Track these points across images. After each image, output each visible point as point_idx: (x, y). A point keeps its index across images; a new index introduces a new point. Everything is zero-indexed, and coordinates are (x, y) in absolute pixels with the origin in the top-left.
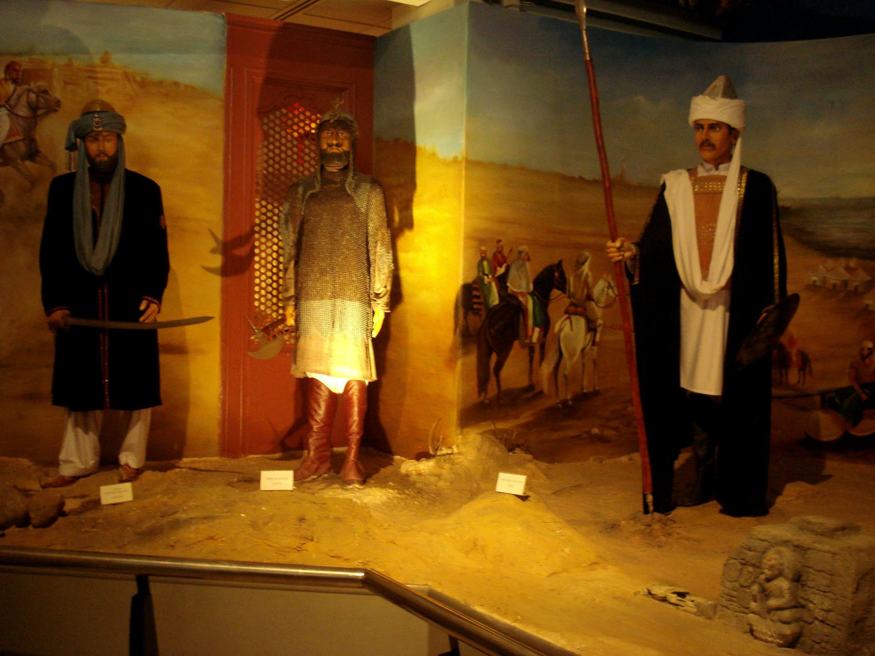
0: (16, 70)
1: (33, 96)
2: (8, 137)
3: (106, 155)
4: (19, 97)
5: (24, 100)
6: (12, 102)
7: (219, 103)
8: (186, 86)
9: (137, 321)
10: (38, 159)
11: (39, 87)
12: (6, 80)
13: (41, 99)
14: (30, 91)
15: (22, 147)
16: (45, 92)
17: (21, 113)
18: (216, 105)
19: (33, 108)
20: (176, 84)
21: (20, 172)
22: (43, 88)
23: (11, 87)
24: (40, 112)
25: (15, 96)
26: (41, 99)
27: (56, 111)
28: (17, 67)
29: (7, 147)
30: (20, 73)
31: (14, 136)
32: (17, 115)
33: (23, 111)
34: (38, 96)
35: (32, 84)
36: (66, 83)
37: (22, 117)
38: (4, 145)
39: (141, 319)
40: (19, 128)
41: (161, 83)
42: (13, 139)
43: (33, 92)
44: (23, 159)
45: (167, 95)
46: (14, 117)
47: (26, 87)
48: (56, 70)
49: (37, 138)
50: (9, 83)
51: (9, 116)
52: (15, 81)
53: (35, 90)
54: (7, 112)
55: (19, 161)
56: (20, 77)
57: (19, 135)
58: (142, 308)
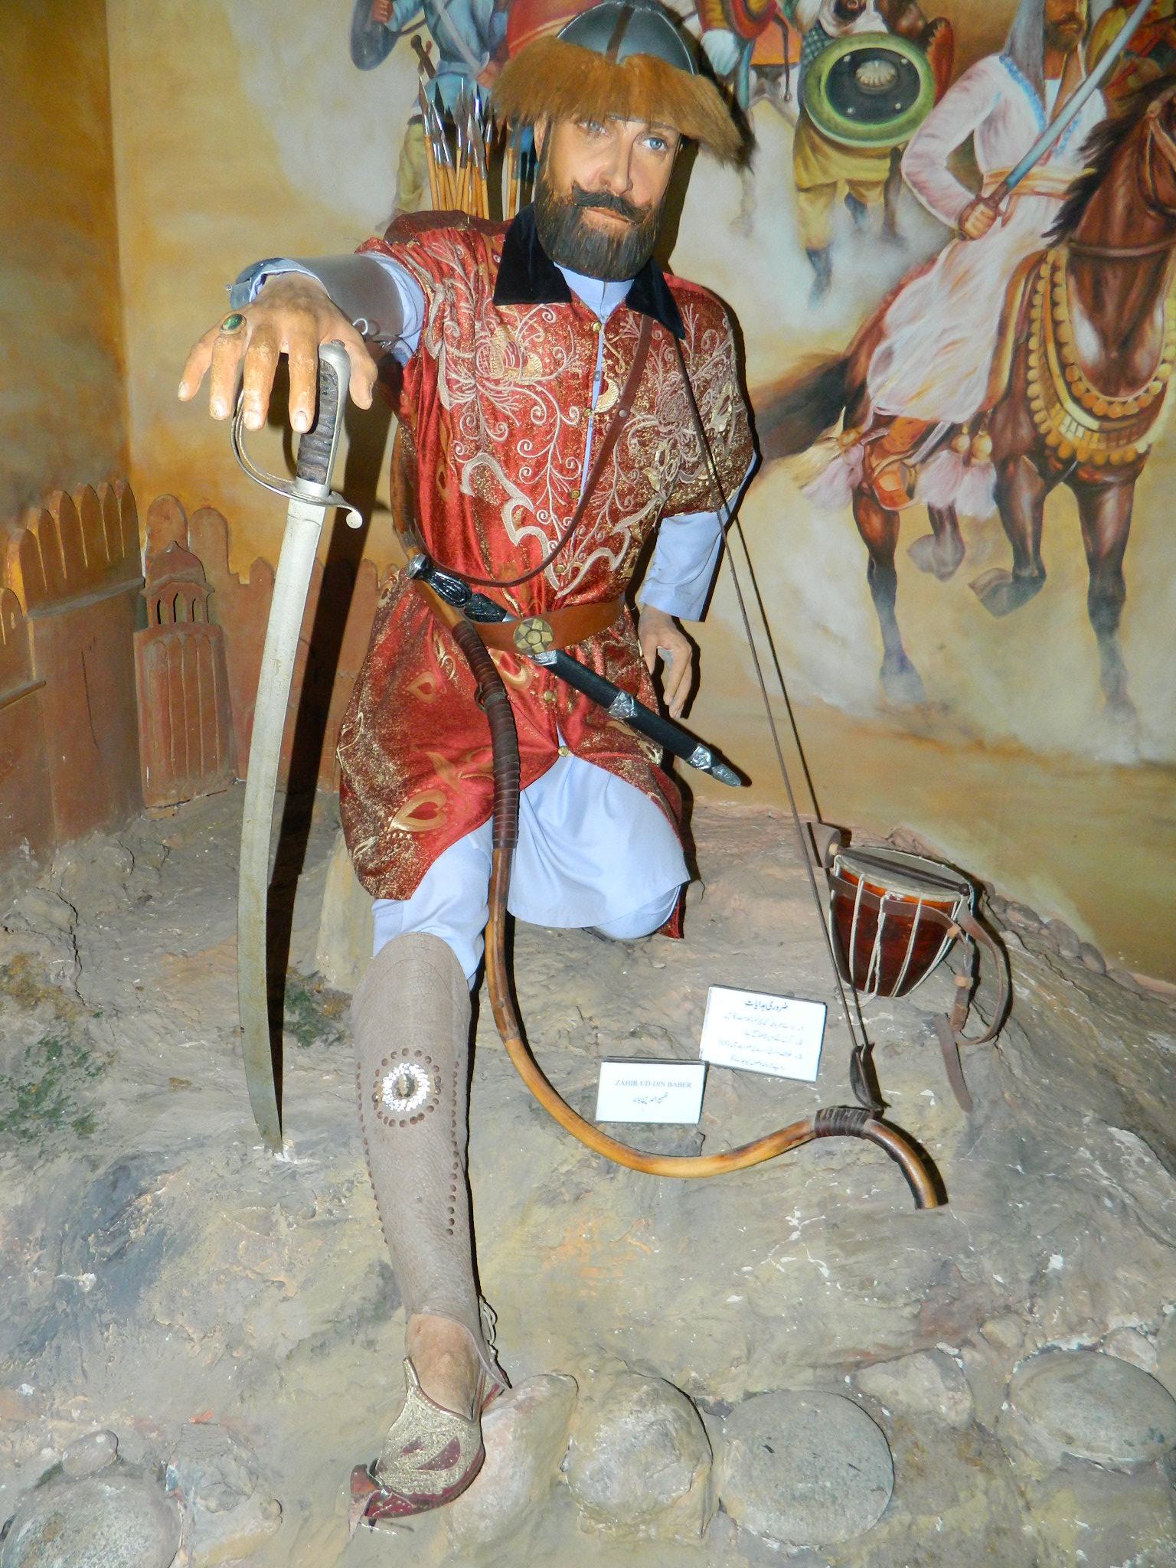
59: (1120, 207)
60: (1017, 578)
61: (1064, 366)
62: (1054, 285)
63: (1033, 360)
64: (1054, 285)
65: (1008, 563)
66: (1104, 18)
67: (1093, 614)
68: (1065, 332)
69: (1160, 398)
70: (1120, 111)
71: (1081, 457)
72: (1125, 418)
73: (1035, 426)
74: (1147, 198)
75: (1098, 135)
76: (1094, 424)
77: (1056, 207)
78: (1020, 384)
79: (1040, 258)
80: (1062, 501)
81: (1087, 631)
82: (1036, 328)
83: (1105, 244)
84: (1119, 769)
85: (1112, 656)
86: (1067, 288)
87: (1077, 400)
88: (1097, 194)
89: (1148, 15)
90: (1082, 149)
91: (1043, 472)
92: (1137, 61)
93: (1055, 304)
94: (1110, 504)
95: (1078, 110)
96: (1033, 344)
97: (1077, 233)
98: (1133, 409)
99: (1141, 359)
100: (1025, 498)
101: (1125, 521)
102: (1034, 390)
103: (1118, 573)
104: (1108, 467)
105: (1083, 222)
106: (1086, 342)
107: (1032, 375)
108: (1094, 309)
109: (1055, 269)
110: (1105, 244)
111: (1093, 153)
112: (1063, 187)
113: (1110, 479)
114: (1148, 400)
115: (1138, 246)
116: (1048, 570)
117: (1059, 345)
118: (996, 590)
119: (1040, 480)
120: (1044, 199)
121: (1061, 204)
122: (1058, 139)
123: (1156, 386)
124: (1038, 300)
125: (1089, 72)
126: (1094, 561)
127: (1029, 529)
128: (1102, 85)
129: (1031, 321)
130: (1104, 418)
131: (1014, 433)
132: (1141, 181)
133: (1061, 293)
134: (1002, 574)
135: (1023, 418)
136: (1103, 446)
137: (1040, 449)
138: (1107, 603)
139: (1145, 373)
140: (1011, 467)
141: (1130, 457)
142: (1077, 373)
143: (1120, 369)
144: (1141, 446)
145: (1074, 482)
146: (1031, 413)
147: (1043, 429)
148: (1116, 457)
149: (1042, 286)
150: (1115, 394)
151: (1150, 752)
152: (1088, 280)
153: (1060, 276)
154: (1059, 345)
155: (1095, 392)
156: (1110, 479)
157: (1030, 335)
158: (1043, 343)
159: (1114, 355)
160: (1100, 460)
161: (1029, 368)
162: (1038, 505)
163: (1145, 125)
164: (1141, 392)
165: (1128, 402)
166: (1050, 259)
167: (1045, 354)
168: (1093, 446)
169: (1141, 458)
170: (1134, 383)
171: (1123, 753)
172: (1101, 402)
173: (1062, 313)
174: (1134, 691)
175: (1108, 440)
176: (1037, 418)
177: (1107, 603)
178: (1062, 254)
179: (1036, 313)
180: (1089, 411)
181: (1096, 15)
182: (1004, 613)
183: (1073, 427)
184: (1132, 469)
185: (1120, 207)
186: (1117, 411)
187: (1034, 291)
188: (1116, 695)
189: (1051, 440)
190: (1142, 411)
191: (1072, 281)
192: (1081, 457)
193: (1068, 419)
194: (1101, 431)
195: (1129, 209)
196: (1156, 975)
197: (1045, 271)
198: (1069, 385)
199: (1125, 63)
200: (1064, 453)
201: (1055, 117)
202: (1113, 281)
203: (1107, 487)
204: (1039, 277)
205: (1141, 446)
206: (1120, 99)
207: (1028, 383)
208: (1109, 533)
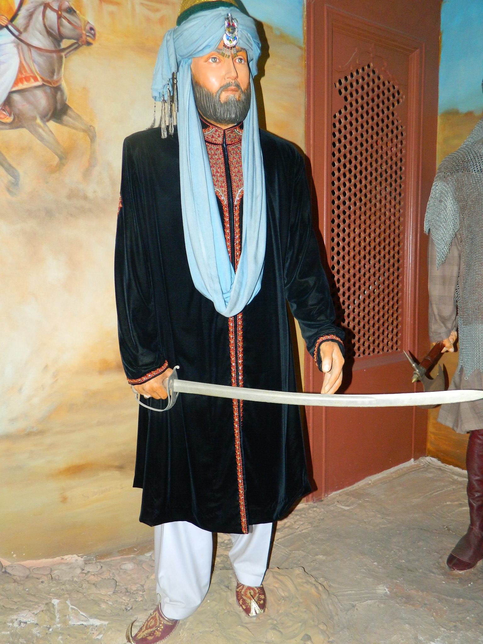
1: (52, 16)
2: (18, 80)
4: (30, 16)
6: (20, 21)
7: (299, 52)
10: (65, 118)
13: (64, 21)
15: (42, 100)
16: (70, 11)
17: (35, 43)
19: (56, 37)
21: (41, 139)
24: (65, 43)
25: (23, 13)
26: (64, 21)
27: (89, 44)
29: (16, 97)
31: (27, 79)
32: (28, 45)
33: (38, 39)
34: (59, 17)
38: (11, 93)
40: (35, 68)
44: (45, 117)
46: (25, 47)
49: (64, 85)
51: (17, 46)
54: (13, 38)
55: (39, 121)
57: (36, 79)
196: (37, 557)
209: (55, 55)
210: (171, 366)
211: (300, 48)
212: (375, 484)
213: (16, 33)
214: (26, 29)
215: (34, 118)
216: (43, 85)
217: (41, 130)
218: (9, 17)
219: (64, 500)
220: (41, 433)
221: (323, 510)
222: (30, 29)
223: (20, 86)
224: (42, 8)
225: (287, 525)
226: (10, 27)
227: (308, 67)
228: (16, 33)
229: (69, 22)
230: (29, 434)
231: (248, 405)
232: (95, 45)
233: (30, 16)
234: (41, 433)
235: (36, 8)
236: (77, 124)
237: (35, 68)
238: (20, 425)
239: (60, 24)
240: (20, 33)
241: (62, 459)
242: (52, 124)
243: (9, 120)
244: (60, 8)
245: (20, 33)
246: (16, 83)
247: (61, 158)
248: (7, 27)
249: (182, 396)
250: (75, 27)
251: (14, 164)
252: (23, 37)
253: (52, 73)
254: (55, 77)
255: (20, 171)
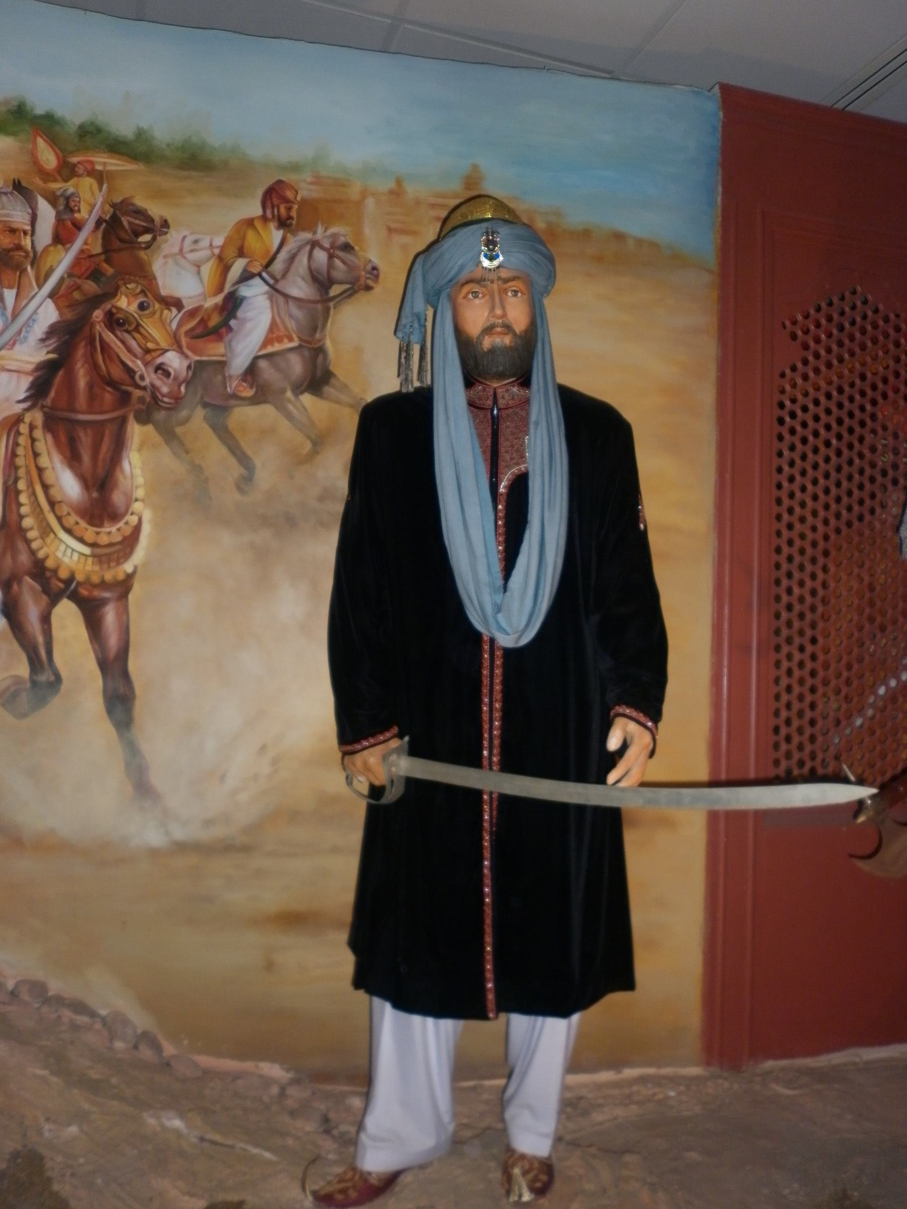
0: (286, 201)
1: (321, 256)
2: (267, 342)
3: (508, 328)
4: (292, 258)
5: (303, 260)
6: (278, 266)
8: (639, 242)
9: (601, 780)
10: (327, 389)
11: (335, 236)
12: (264, 219)
13: (337, 262)
14: (314, 244)
15: (297, 366)
16: (347, 247)
17: (295, 292)
18: (701, 284)
19: (322, 282)
20: (619, 237)
21: (289, 416)
22: (342, 240)
23: (276, 235)
24: (335, 290)
25: (283, 255)
26: (337, 262)
27: (368, 288)
28: (289, 194)
29: (263, 364)
30: (295, 207)
31: (279, 340)
32: (286, 296)
33: (299, 287)
34: (331, 257)
35: (320, 230)
36: (390, 230)
37: (297, 300)
38: (257, 358)
39: (612, 777)
41: (585, 234)
42: (277, 347)
43: (322, 248)
44: (298, 389)
45: (599, 259)
46: (281, 299)
47: (306, 236)
48: (370, 202)
49: (328, 344)
50: (272, 225)
51: (271, 298)
52: (283, 224)
53: (327, 245)
54: (266, 288)
55: (289, 394)
56: (294, 214)
57: (291, 339)
58: (613, 743)
59: (82, 382)
60: (34, 683)
61: (52, 504)
62: (33, 440)
63: (23, 498)
64: (33, 440)
65: (23, 669)
66: (46, 249)
67: (110, 711)
68: (49, 477)
69: (137, 529)
70: (69, 315)
71: (80, 577)
72: (110, 545)
73: (33, 553)
74: (102, 377)
75: (52, 331)
76: (87, 550)
77: (25, 382)
78: (14, 517)
79: (18, 419)
80: (67, 615)
81: (106, 728)
82: (22, 472)
83: (74, 410)
84: (154, 853)
85: (132, 749)
86: (45, 443)
87: (69, 531)
88: (61, 373)
89: (82, 251)
90: (43, 340)
91: (46, 590)
92: (78, 281)
93: (36, 455)
94: (110, 616)
95: (35, 312)
96: (21, 485)
97: (48, 401)
98: (118, 538)
99: (117, 498)
100: (32, 612)
101: (125, 631)
102: (27, 522)
103: (126, 675)
104: (103, 585)
105: (52, 394)
106: (69, 485)
107: (24, 510)
108: (73, 459)
109: (32, 428)
110: (74, 410)
111: (53, 343)
112: (30, 367)
113: (106, 595)
114: (128, 531)
115: (102, 413)
116: (64, 674)
117: (46, 487)
118: (15, 695)
119: (45, 599)
120: (15, 375)
121: (31, 379)
122: (20, 331)
123: (134, 520)
124: (20, 451)
125: (40, 287)
126: (103, 665)
127: (40, 639)
128: (52, 295)
129: (17, 468)
130: (93, 545)
131: (14, 557)
132: (95, 366)
133: (41, 446)
134: (18, 680)
135: (21, 545)
136: (97, 568)
137: (40, 571)
138: (120, 700)
139: (122, 509)
140: (15, 587)
141: (121, 576)
142: (65, 510)
143: (101, 505)
144: (128, 567)
145: (75, 597)
146: (28, 542)
147: (41, 554)
148: (108, 576)
149: (22, 440)
150: (101, 525)
151: (179, 834)
152: (63, 438)
153: (38, 433)
154: (46, 487)
155: (83, 524)
156: (106, 595)
157: (17, 480)
158: (30, 484)
159: (95, 495)
160: (95, 579)
161: (20, 505)
162: (46, 619)
163: (92, 326)
164: (121, 524)
165: (111, 532)
166: (28, 418)
167: (34, 494)
168: (89, 567)
169: (130, 577)
170: (115, 517)
171: (154, 837)
172: (90, 533)
173: (44, 461)
174: (157, 779)
175: (100, 563)
176: (34, 545)
177: (120, 700)
178: (38, 417)
179: (20, 461)
180: (81, 540)
181: (40, 248)
182: (24, 715)
183: (68, 553)
184: (124, 586)
185: (82, 382)
186: (104, 540)
187: (16, 444)
188: (141, 786)
189: (50, 563)
190: (125, 539)
191: (49, 437)
192: (80, 577)
193: (62, 547)
194: (93, 555)
195: (90, 387)
196: (218, 1054)
197: (24, 428)
198: (59, 519)
199: (68, 282)
200: (63, 574)
201: (15, 316)
202: (85, 440)
203: (104, 602)
204: (18, 433)
205: (128, 567)
206: (70, 306)
207: (21, 517)
208: (113, 641)
209: (319, 307)
210: (400, 736)
211: (709, 271)
212: (869, 1067)
213: (271, 282)
214: (284, 275)
215: (283, 391)
216: (300, 346)
217: (290, 407)
218: (264, 262)
219: (270, 966)
220: (246, 849)
221: (736, 1086)
222: (290, 275)
223: (270, 349)
224: (308, 248)
225: (656, 1098)
226: (264, 275)
227: (723, 300)
228: (271, 282)
229: (344, 262)
230: (225, 848)
231: (508, 803)
232: (378, 290)
233: (292, 258)
234: (246, 849)
235: (300, 249)
236: (344, 398)
237: (291, 325)
238: (218, 832)
239: (330, 265)
240: (277, 281)
241: (271, 899)
242: (307, 399)
243: (249, 393)
244: (333, 246)
245: (277, 281)
246: (264, 345)
247: (315, 444)
248: (260, 275)
249: (410, 782)
250: (351, 268)
251: (249, 452)
252: (279, 286)
253: (314, 329)
254: (318, 335)
255: (258, 462)
